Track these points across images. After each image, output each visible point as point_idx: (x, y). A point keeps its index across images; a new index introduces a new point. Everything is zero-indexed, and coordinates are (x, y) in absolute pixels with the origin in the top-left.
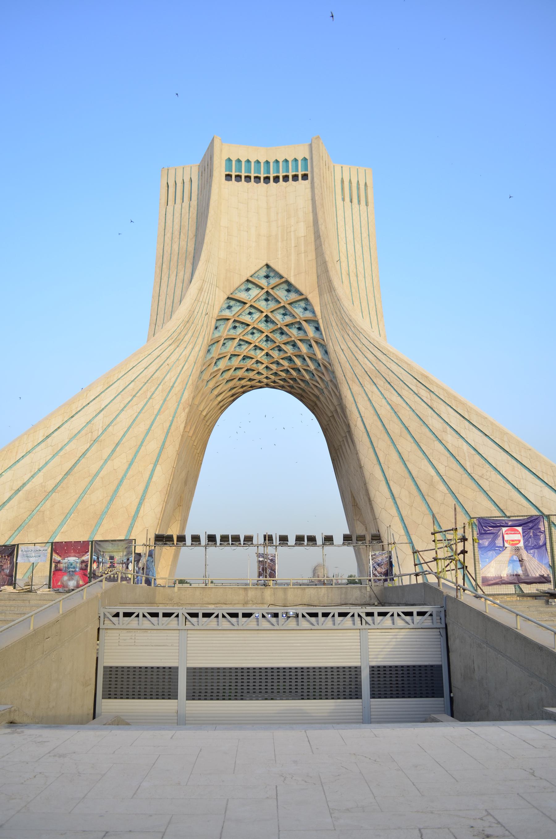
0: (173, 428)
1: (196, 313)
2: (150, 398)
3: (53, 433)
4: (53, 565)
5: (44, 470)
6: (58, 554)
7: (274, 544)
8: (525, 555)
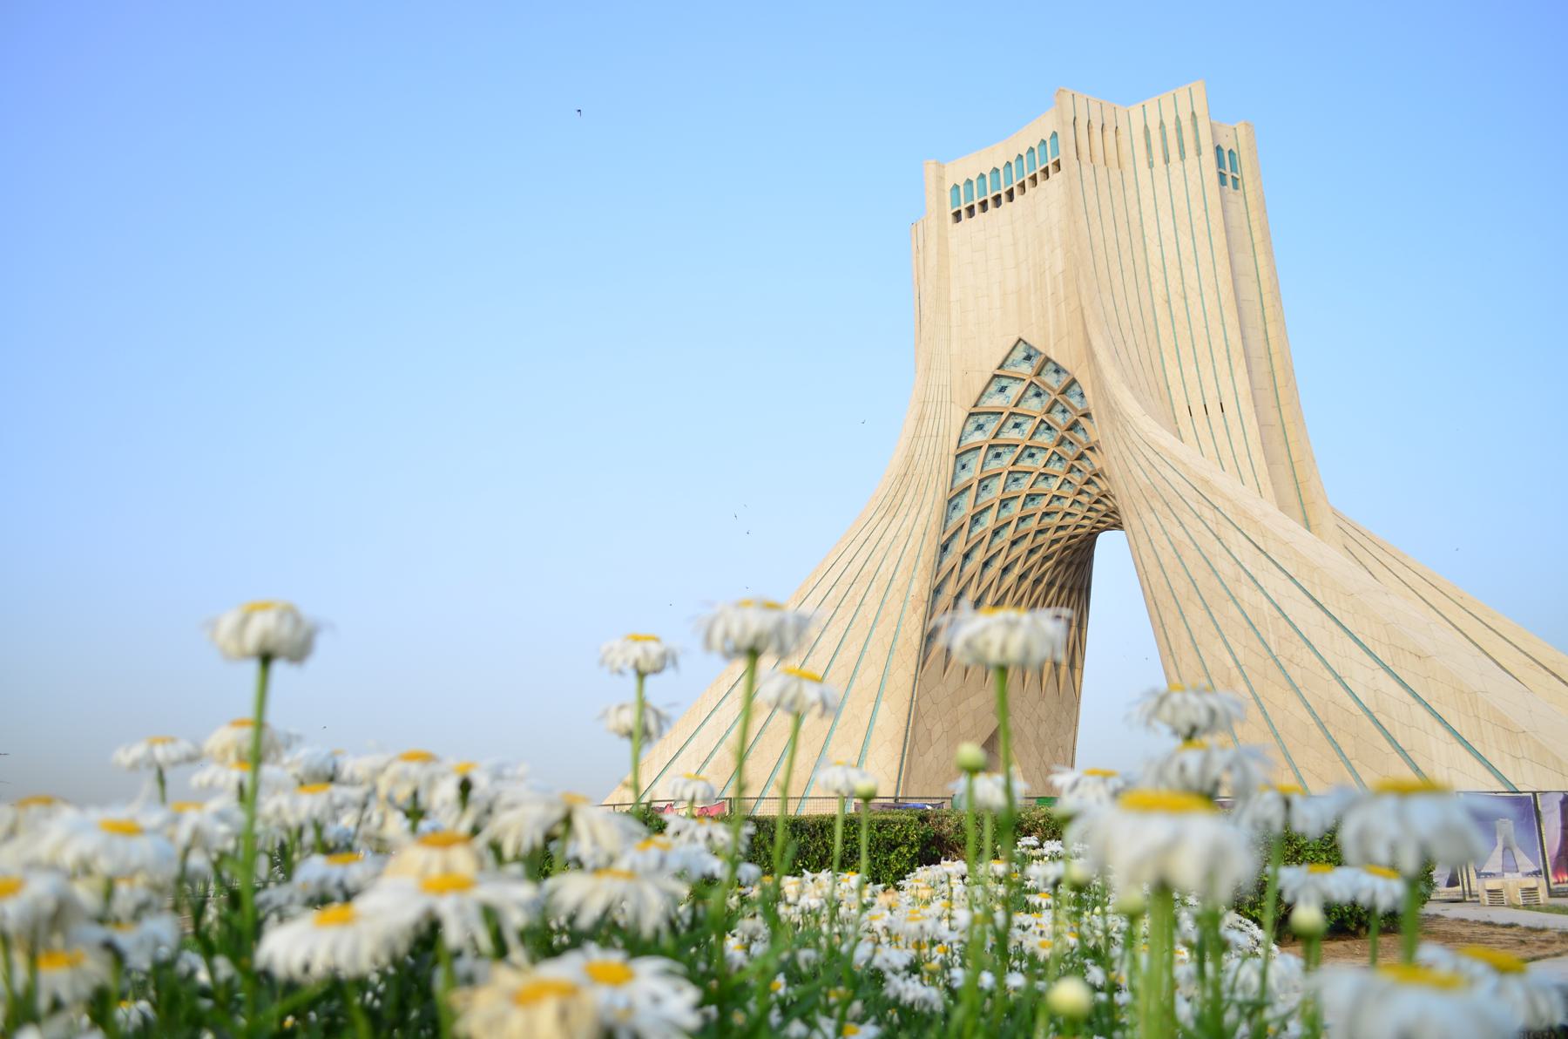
0: (899, 642)
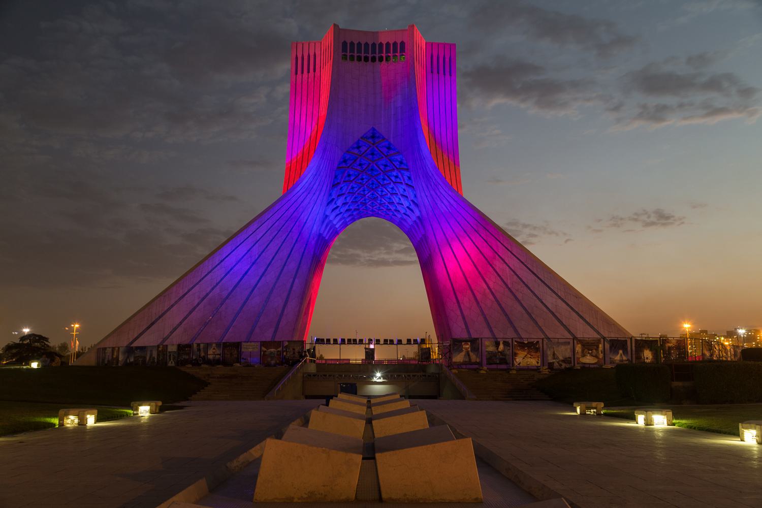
3: (225, 258)
4: (262, 353)
6: (265, 347)
8: (470, 353)
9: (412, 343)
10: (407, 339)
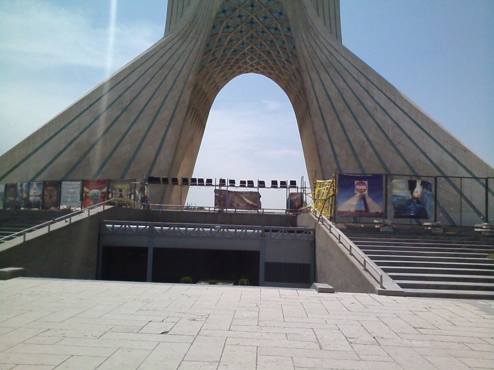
1: (199, 14)
2: (164, 79)
5: (89, 129)
7: (226, 185)
9: (279, 185)
10: (272, 181)
